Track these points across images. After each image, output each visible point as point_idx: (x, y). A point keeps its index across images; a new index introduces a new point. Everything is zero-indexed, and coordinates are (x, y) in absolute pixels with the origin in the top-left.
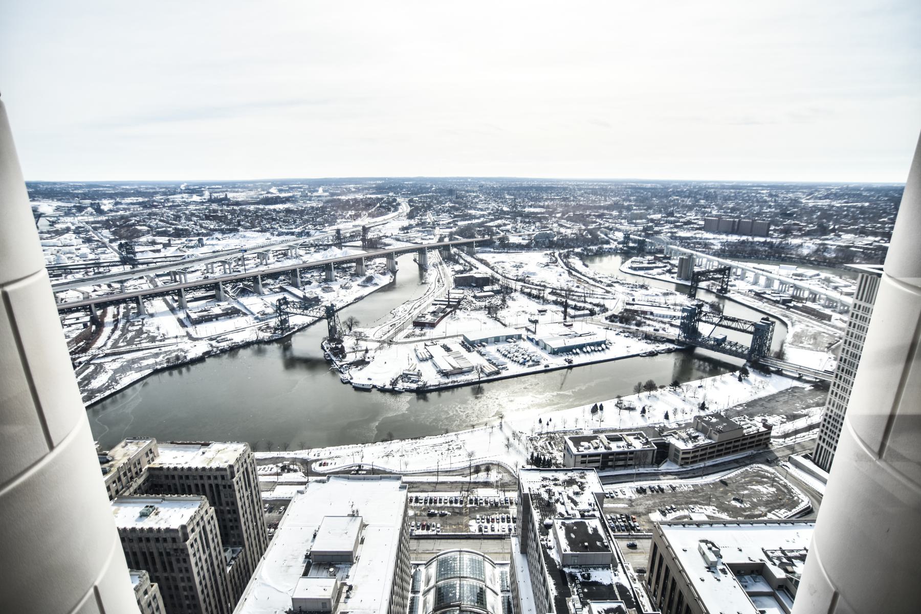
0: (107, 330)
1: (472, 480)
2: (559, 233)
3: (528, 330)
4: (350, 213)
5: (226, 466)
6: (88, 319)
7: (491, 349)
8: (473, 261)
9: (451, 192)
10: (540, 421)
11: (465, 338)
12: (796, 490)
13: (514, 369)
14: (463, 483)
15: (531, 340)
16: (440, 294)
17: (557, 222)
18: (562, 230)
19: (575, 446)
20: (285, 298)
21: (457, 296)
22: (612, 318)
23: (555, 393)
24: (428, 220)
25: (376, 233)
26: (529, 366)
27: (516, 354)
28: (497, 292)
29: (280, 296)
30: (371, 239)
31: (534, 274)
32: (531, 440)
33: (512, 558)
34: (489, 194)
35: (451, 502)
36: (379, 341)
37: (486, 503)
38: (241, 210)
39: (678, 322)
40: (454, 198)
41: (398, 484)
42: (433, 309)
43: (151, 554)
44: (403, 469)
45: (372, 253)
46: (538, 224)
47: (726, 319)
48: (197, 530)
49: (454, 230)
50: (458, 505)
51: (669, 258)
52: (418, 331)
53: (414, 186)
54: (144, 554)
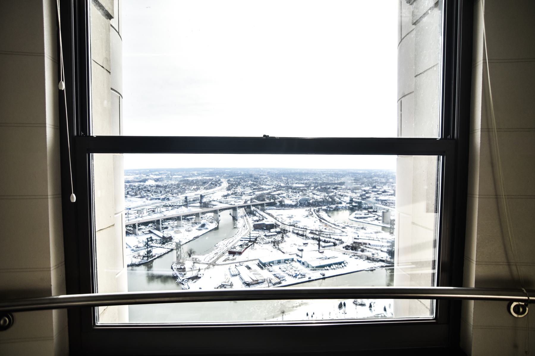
2: (313, 198)
3: (298, 255)
7: (275, 268)
9: (251, 176)
10: (307, 315)
15: (300, 262)
17: (312, 192)
18: (315, 196)
20: (151, 237)
21: (255, 235)
22: (347, 247)
24: (239, 191)
26: (299, 278)
28: (279, 233)
29: (149, 236)
30: (205, 202)
31: (300, 222)
36: (207, 264)
38: (130, 186)
39: (385, 249)
40: (253, 179)
42: (241, 243)
45: (205, 210)
46: (301, 193)
49: (253, 196)
51: (376, 212)
52: (231, 257)
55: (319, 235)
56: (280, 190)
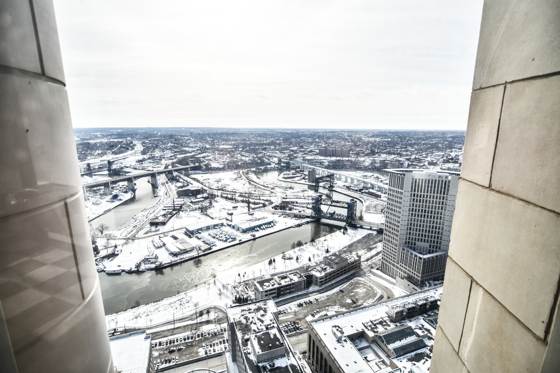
1: (198, 322)
2: (241, 160)
3: (227, 220)
4: (97, 152)
7: (205, 235)
9: (171, 136)
10: (239, 275)
11: (187, 230)
12: (375, 288)
13: (220, 245)
14: (192, 325)
15: (230, 226)
16: (168, 202)
17: (240, 153)
18: (243, 158)
19: (261, 286)
21: (180, 203)
22: (276, 208)
23: (247, 256)
24: (157, 155)
25: (118, 165)
26: (230, 242)
27: (221, 235)
28: (206, 198)
30: (115, 169)
31: (228, 185)
32: (234, 288)
33: (227, 366)
34: (197, 138)
35: (185, 339)
36: (125, 239)
37: (209, 334)
39: (310, 206)
40: (173, 140)
41: (144, 336)
42: (164, 212)
44: (149, 324)
45: (116, 178)
46: (228, 155)
47: (334, 202)
49: (175, 160)
50: (190, 340)
51: (303, 171)
52: (153, 228)
53: (144, 133)
55: (249, 197)
56: (205, 152)
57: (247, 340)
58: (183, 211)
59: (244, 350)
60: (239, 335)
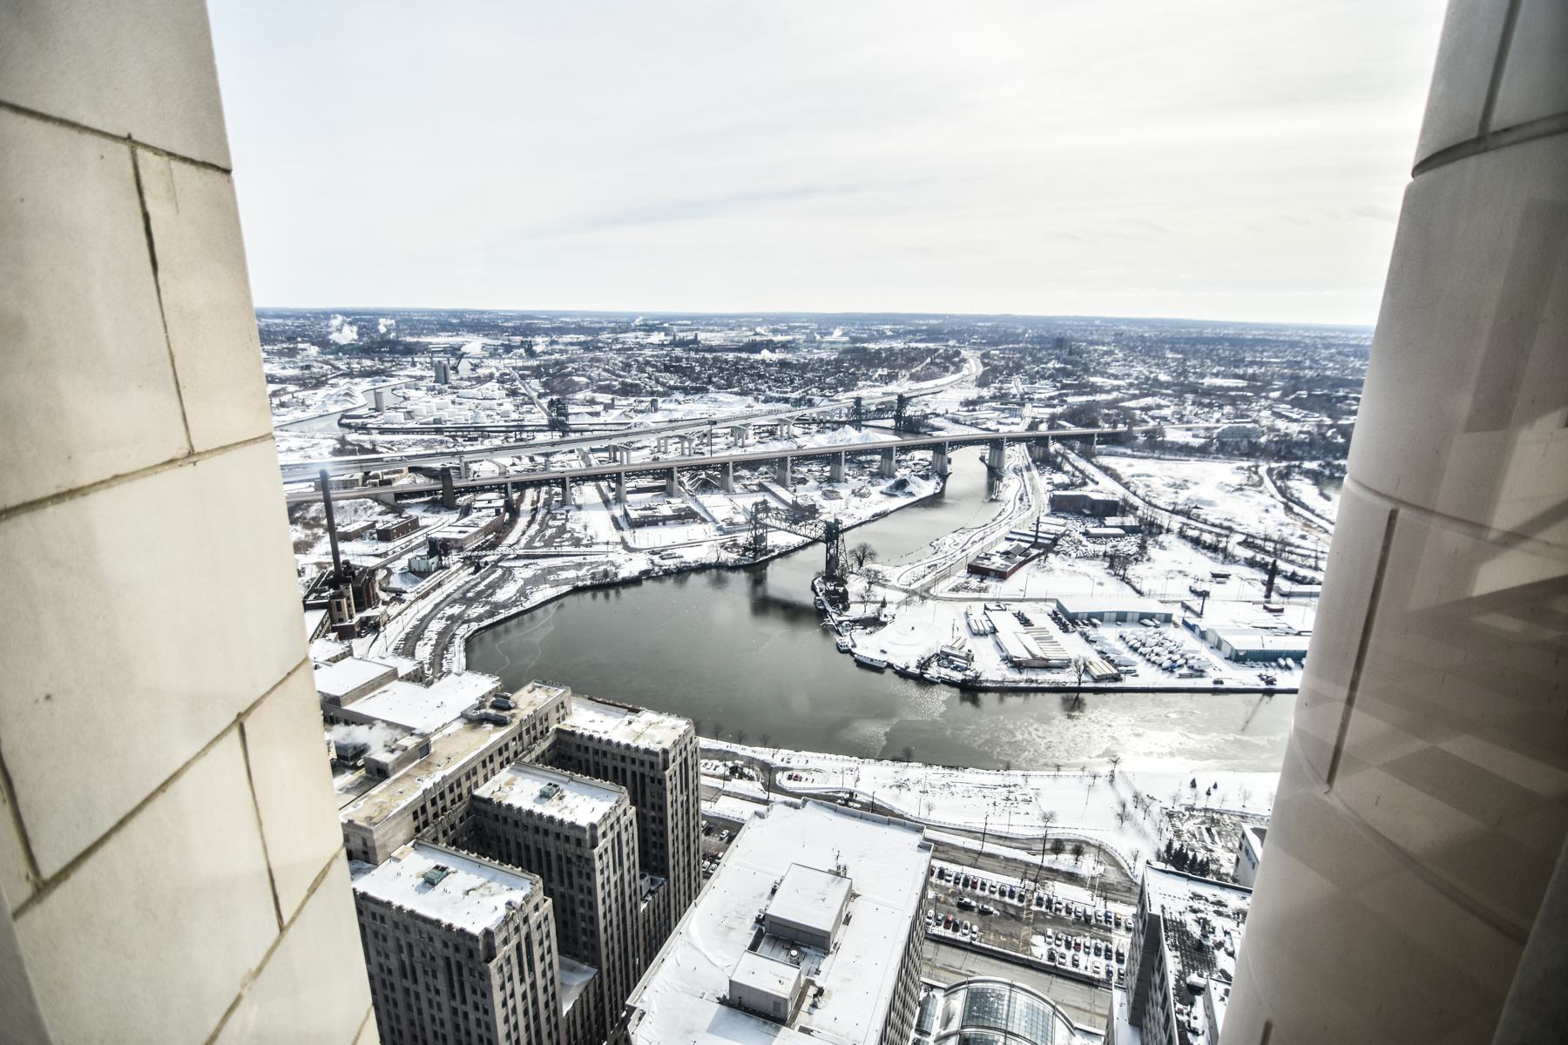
0: (522, 521)
1: (1046, 864)
2: (1272, 429)
3: (1187, 608)
4: (880, 371)
5: (658, 748)
6: (501, 503)
7: (1108, 634)
8: (1090, 469)
9: (1060, 343)
10: (1193, 784)
11: (1060, 606)
13: (1148, 676)
14: (1027, 864)
15: (1192, 628)
16: (1022, 522)
17: (1270, 407)
18: (1281, 424)
20: (765, 502)
21: (1053, 529)
23: (1231, 737)
24: (1014, 391)
25: (919, 407)
26: (1181, 676)
28: (1131, 530)
29: (759, 498)
30: (910, 417)
31: (1210, 504)
32: (1171, 815)
33: (1109, 1027)
34: (1133, 349)
35: (1002, 893)
36: (905, 591)
37: (1069, 911)
38: (715, 359)
41: (917, 839)
42: (1005, 546)
43: (548, 854)
44: (924, 814)
45: (910, 440)
46: (1228, 409)
48: (610, 835)
49: (1059, 410)
50: (1015, 902)
52: (974, 582)
53: (993, 330)
54: (539, 851)
55: (1275, 554)
56: (1153, 395)
57: (1195, 990)
58: (1057, 553)
59: (1180, 1012)
60: (1172, 962)
